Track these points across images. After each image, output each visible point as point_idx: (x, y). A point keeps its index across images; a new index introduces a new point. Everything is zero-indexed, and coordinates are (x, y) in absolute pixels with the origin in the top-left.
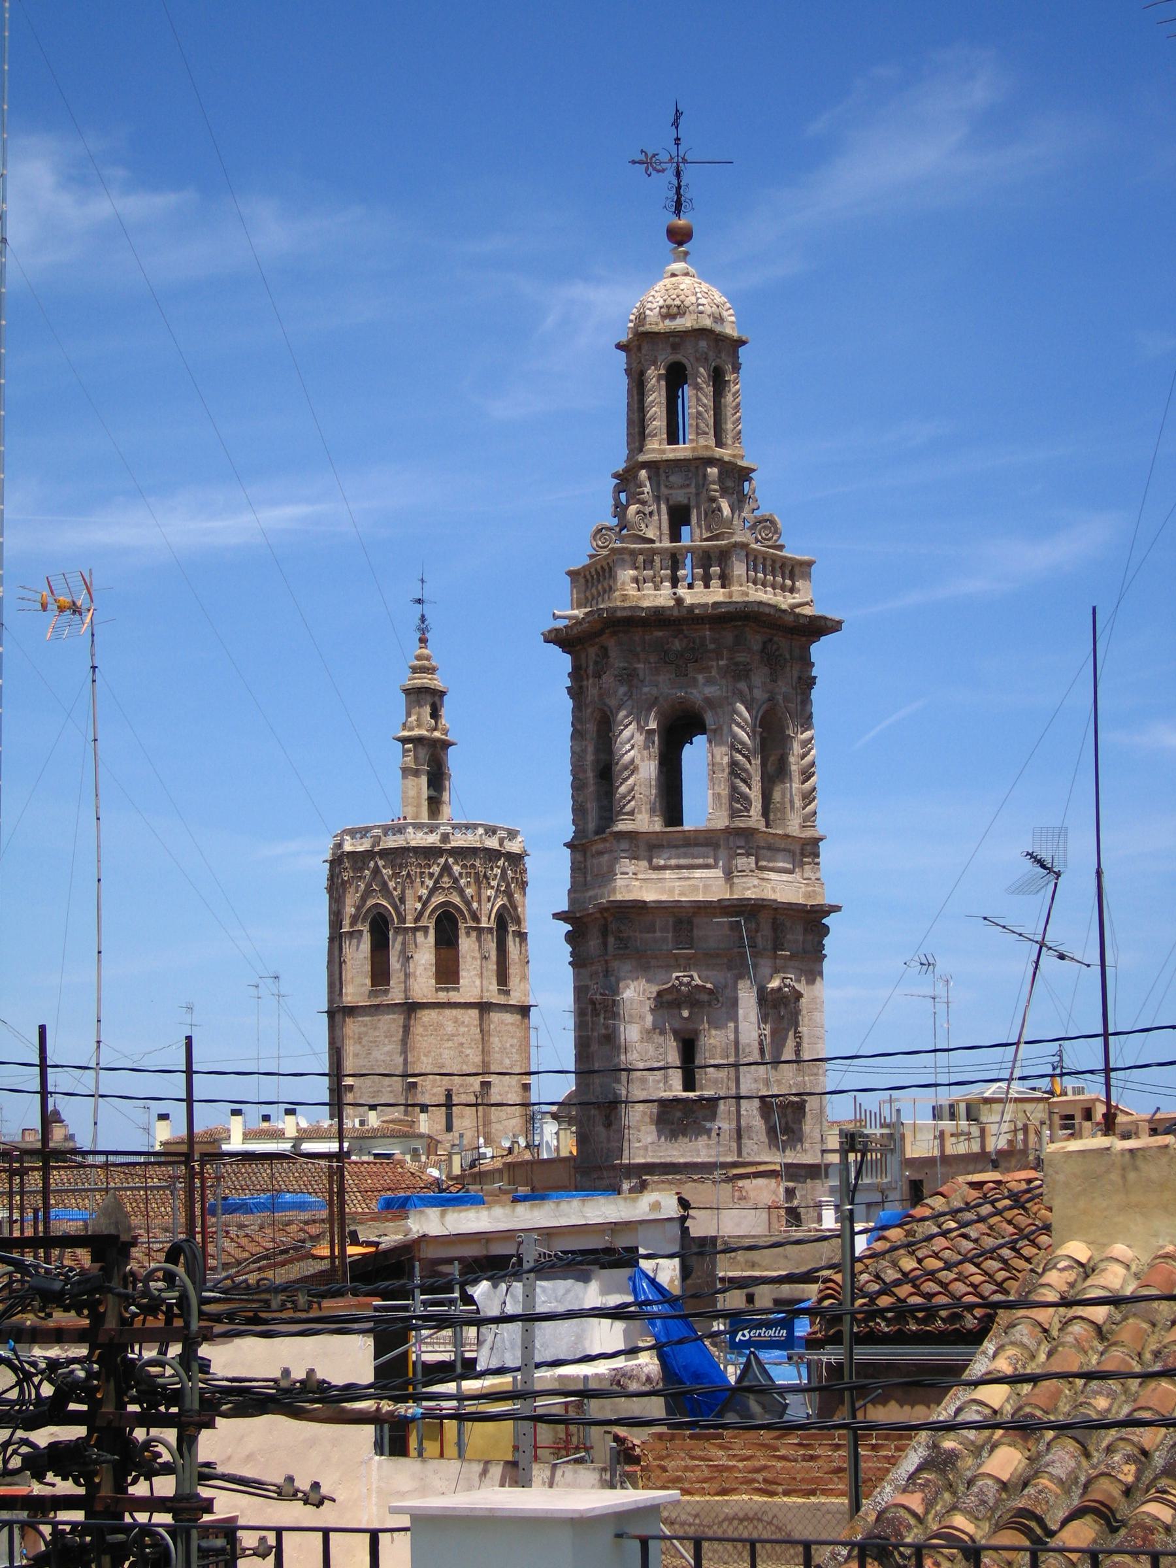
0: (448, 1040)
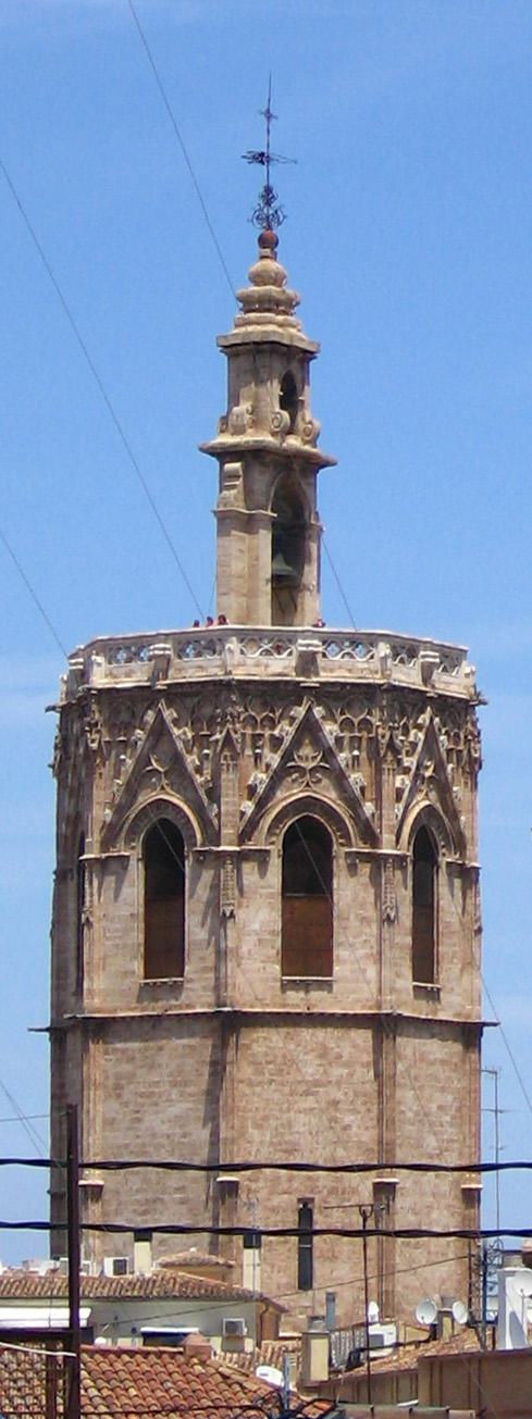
0: (307, 1093)
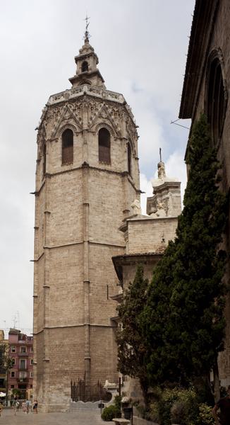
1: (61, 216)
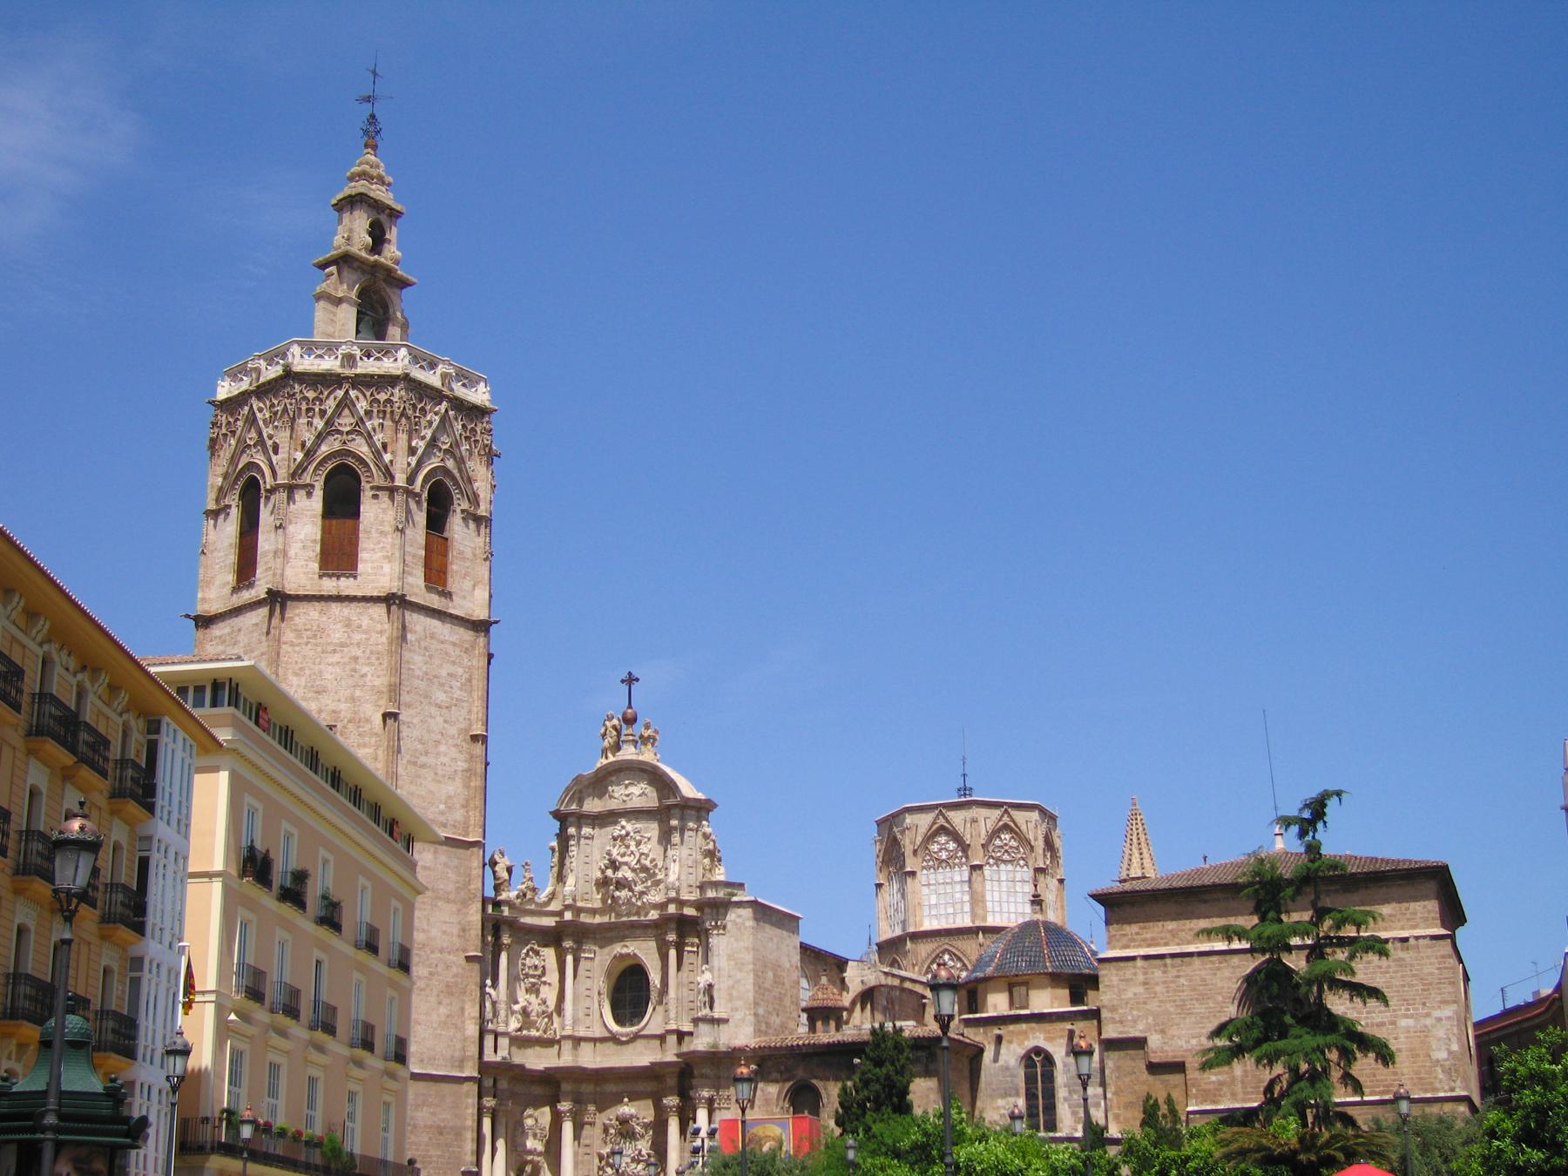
0: (334, 651)
1: (420, 741)
